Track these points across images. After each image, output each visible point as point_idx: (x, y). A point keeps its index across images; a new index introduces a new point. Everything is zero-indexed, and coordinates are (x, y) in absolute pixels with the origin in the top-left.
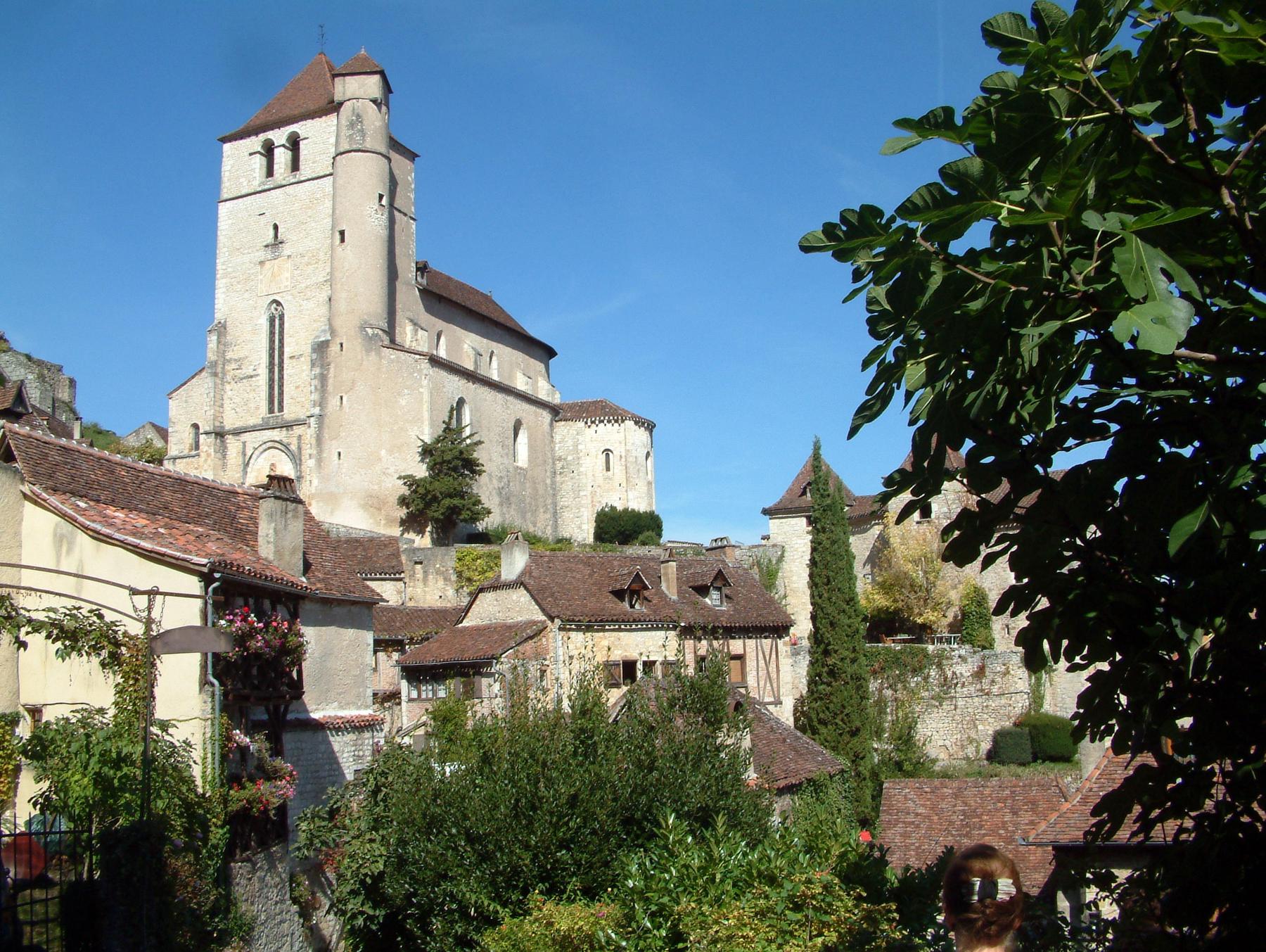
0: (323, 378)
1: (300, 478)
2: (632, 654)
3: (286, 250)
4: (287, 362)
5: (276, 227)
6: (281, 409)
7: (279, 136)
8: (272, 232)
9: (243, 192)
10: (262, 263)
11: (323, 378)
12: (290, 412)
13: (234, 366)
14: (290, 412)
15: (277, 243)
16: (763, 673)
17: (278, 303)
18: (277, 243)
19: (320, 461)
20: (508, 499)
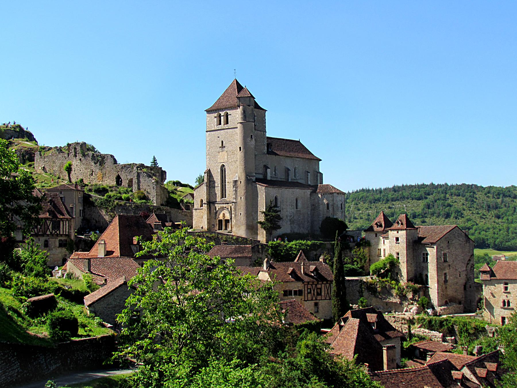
0: (236, 191)
1: (231, 218)
2: (291, 289)
3: (225, 149)
4: (227, 183)
5: (222, 142)
6: (225, 197)
7: (222, 113)
8: (221, 143)
9: (213, 129)
10: (219, 152)
11: (236, 191)
12: (227, 199)
13: (212, 183)
14: (227, 199)
15: (223, 147)
16: (326, 292)
17: (223, 166)
18: (223, 147)
19: (235, 215)
20: (293, 222)
